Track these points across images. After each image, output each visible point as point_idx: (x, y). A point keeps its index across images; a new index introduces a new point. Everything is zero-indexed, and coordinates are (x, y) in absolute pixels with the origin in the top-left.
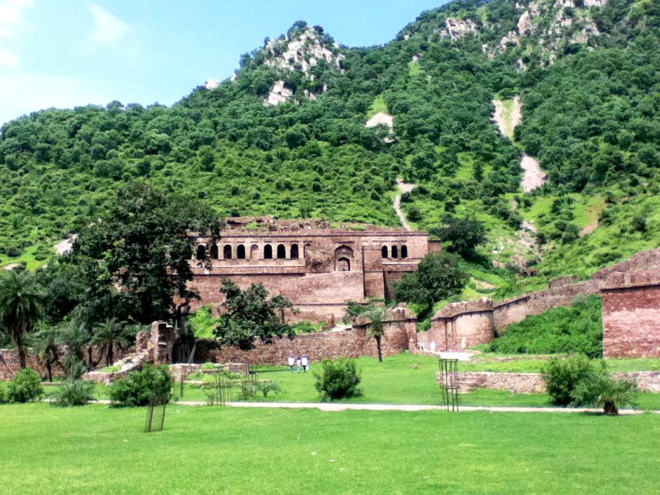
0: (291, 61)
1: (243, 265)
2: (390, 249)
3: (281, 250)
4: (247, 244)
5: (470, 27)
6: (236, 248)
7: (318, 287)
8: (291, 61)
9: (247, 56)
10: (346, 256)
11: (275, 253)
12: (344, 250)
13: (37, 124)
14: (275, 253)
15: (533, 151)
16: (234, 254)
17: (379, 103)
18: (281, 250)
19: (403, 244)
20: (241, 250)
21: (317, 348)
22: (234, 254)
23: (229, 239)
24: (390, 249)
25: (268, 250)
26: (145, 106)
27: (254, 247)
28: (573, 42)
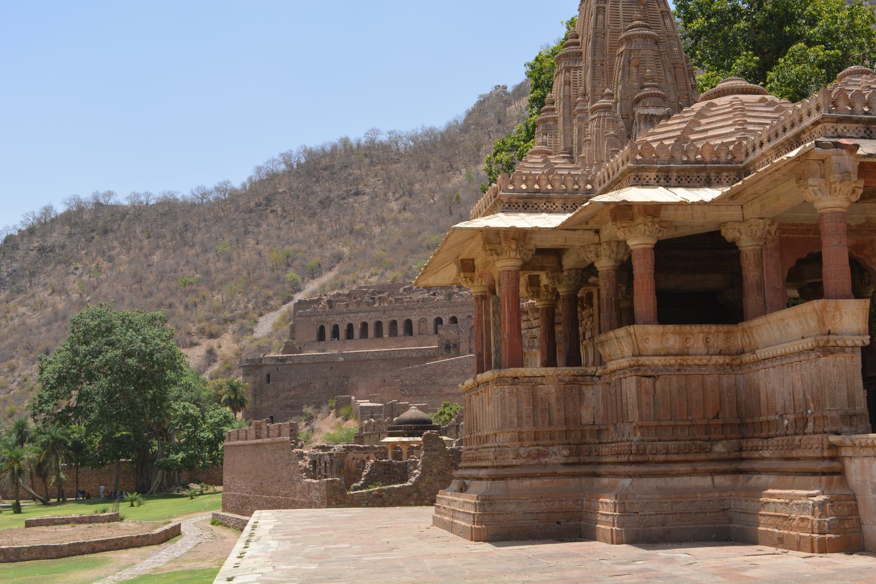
1: (410, 346)
4: (415, 319)
16: (401, 330)
20: (409, 324)
27: (423, 321)
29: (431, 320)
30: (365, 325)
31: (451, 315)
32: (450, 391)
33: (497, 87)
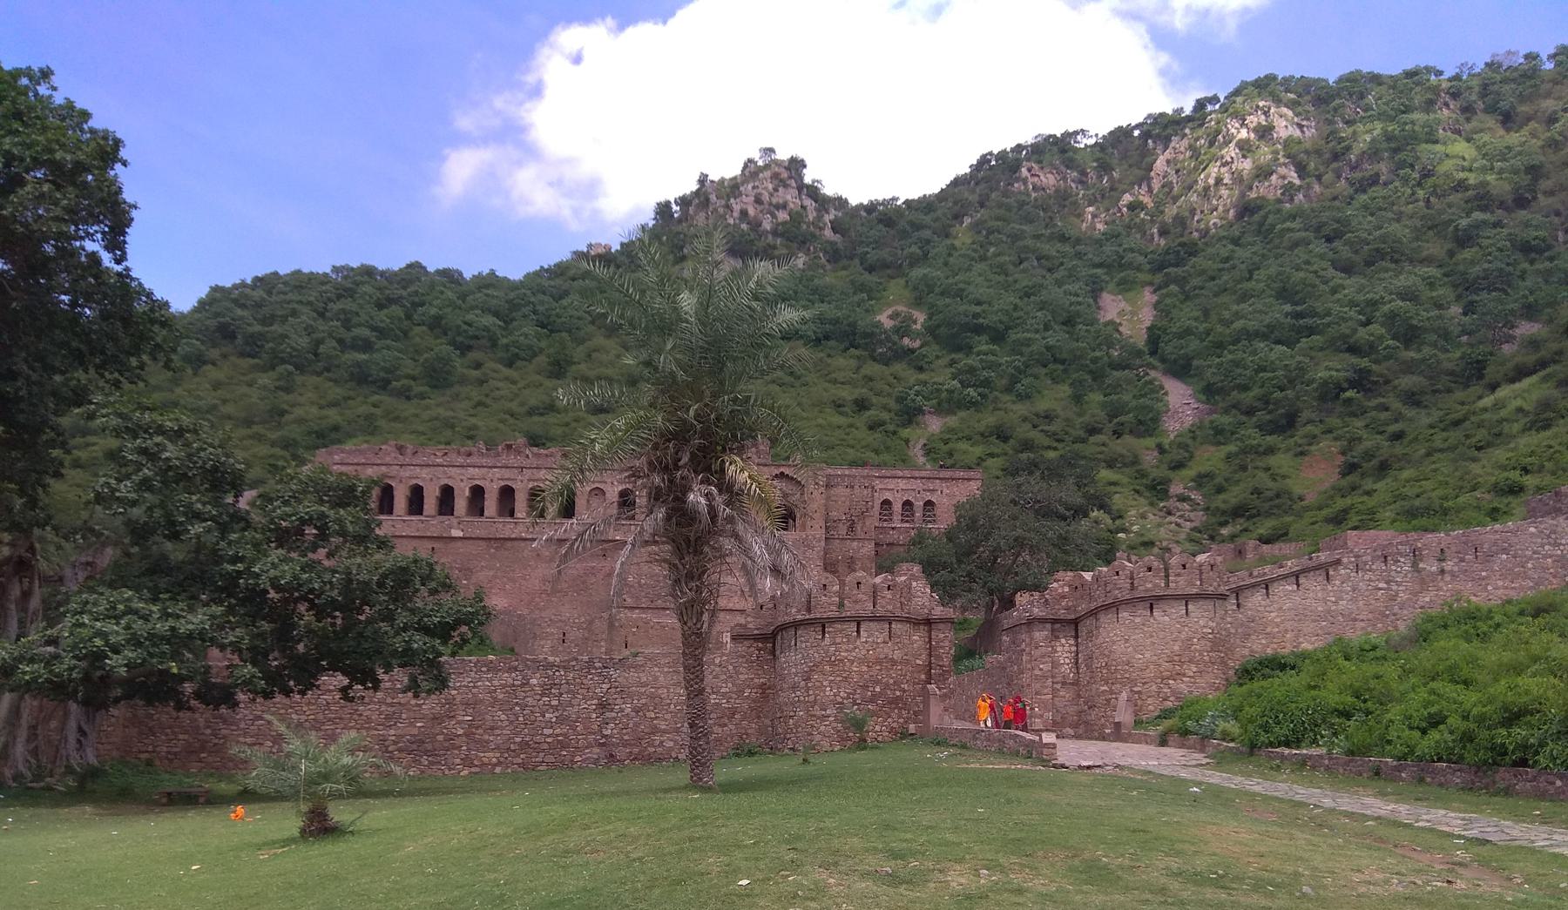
2: (897, 507)
5: (1064, 179)
8: (744, 213)
13: (258, 294)
17: (896, 289)
19: (928, 496)
23: (542, 474)
24: (897, 507)
26: (468, 275)
28: (1253, 195)
29: (612, 493)
30: (478, 493)
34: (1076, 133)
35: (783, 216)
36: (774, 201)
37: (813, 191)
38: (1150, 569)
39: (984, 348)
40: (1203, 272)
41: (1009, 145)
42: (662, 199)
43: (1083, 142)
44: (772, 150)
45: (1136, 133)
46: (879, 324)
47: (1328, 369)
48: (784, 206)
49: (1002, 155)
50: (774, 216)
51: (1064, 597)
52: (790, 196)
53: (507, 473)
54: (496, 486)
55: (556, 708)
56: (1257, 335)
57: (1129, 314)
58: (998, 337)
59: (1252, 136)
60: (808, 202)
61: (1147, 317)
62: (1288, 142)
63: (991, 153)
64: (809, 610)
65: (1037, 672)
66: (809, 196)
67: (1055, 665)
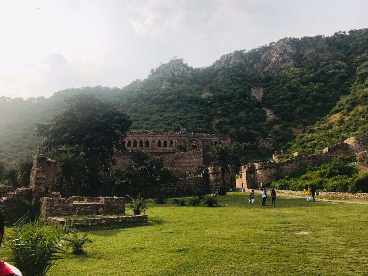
0: (171, 72)
3: (165, 142)
4: (150, 140)
5: (241, 61)
6: (145, 143)
7: (182, 158)
9: (153, 69)
10: (195, 144)
11: (162, 144)
12: (194, 142)
14: (162, 144)
15: (269, 107)
16: (144, 145)
18: (165, 142)
19: (220, 140)
20: (147, 143)
21: (183, 186)
22: (144, 145)
23: (142, 138)
25: (159, 142)
31: (165, 140)
32: (185, 165)
33: (138, 79)
34: (243, 50)
35: (179, 72)
36: (177, 69)
37: (186, 66)
38: (265, 163)
39: (227, 103)
40: (273, 84)
41: (228, 53)
42: (152, 68)
43: (245, 53)
44: (176, 57)
45: (257, 50)
46: (203, 99)
47: (300, 108)
48: (179, 70)
49: (227, 56)
50: (178, 72)
51: (252, 167)
52: (181, 68)
53: (135, 138)
54: (133, 141)
55: (176, 187)
56: (283, 100)
57: (258, 94)
58: (229, 100)
59: (283, 52)
60: (185, 69)
61: (261, 94)
62: (290, 53)
63: (224, 55)
64: (215, 171)
65: (248, 179)
66: (185, 67)
67: (251, 178)
